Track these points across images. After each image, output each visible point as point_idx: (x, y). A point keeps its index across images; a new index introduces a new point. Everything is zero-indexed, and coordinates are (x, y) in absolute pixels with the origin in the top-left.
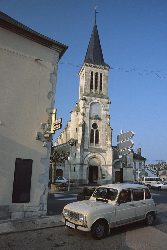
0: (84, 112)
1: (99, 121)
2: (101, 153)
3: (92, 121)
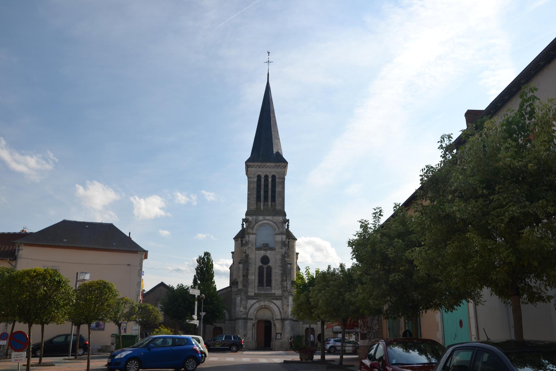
0: (248, 241)
1: (271, 252)
2: (274, 301)
3: (260, 253)
